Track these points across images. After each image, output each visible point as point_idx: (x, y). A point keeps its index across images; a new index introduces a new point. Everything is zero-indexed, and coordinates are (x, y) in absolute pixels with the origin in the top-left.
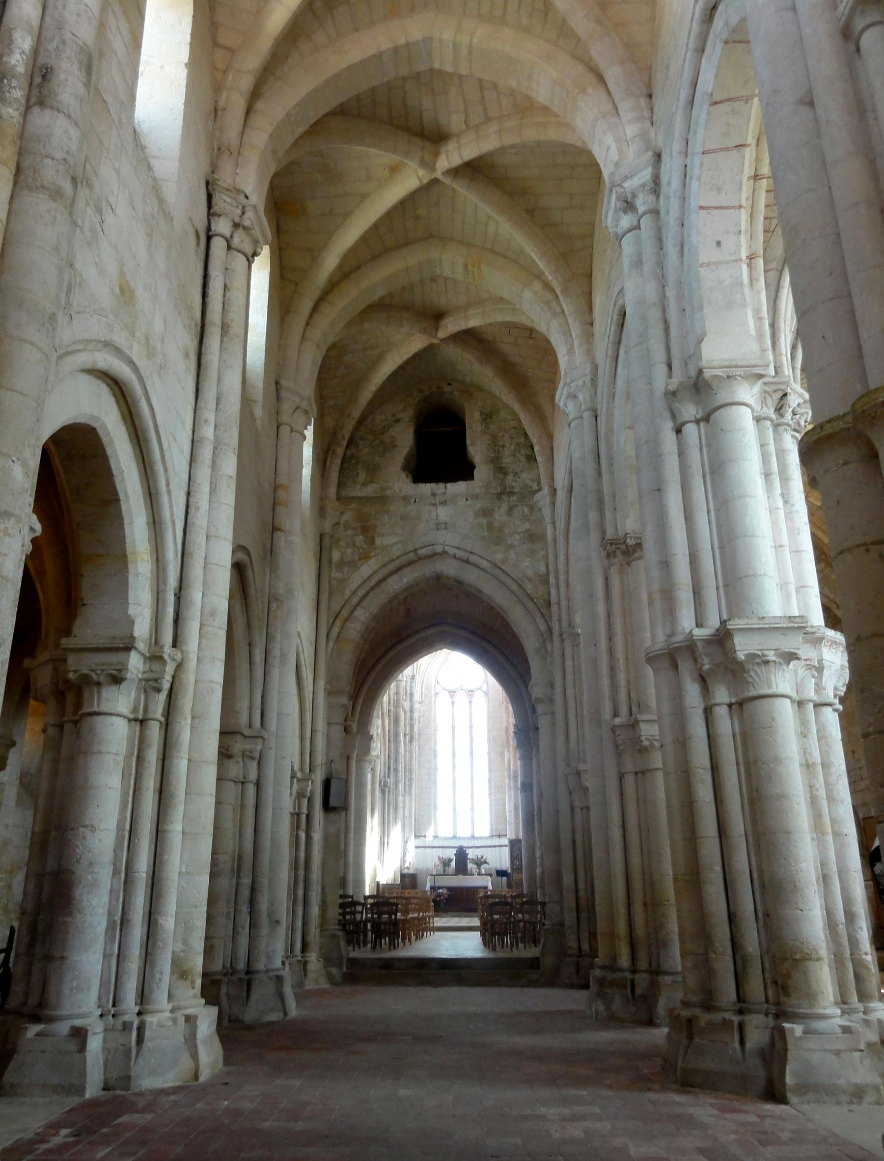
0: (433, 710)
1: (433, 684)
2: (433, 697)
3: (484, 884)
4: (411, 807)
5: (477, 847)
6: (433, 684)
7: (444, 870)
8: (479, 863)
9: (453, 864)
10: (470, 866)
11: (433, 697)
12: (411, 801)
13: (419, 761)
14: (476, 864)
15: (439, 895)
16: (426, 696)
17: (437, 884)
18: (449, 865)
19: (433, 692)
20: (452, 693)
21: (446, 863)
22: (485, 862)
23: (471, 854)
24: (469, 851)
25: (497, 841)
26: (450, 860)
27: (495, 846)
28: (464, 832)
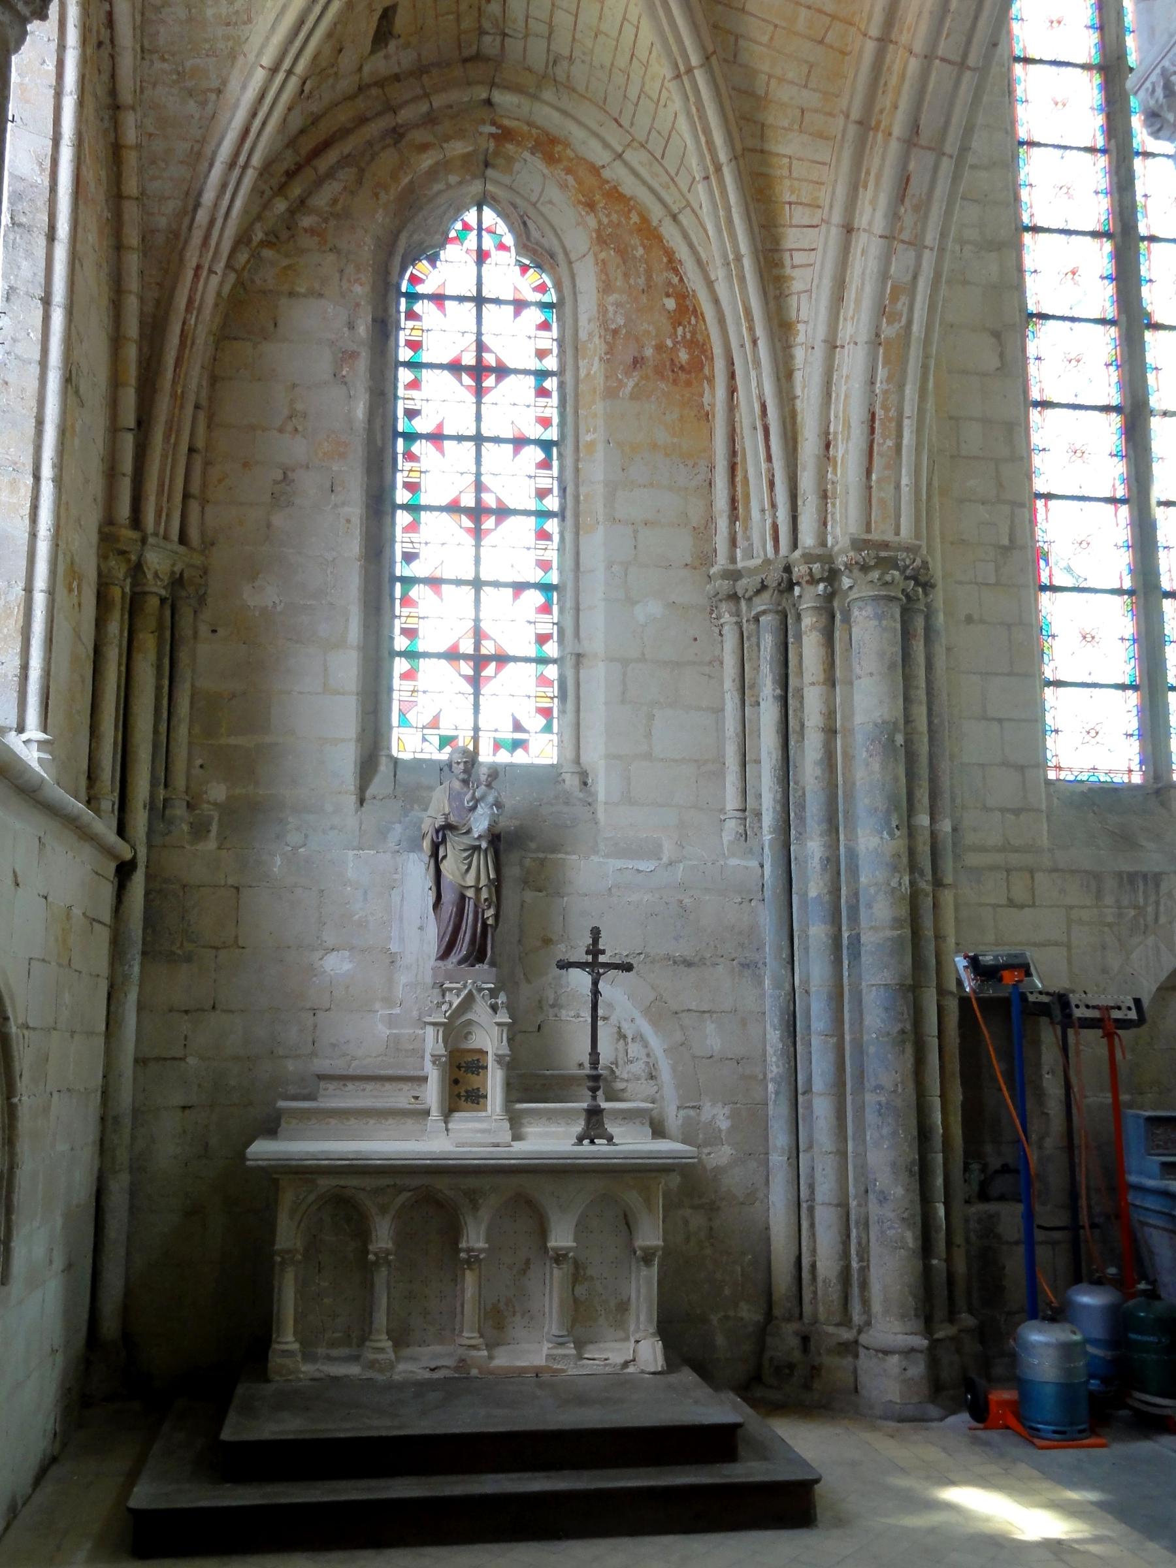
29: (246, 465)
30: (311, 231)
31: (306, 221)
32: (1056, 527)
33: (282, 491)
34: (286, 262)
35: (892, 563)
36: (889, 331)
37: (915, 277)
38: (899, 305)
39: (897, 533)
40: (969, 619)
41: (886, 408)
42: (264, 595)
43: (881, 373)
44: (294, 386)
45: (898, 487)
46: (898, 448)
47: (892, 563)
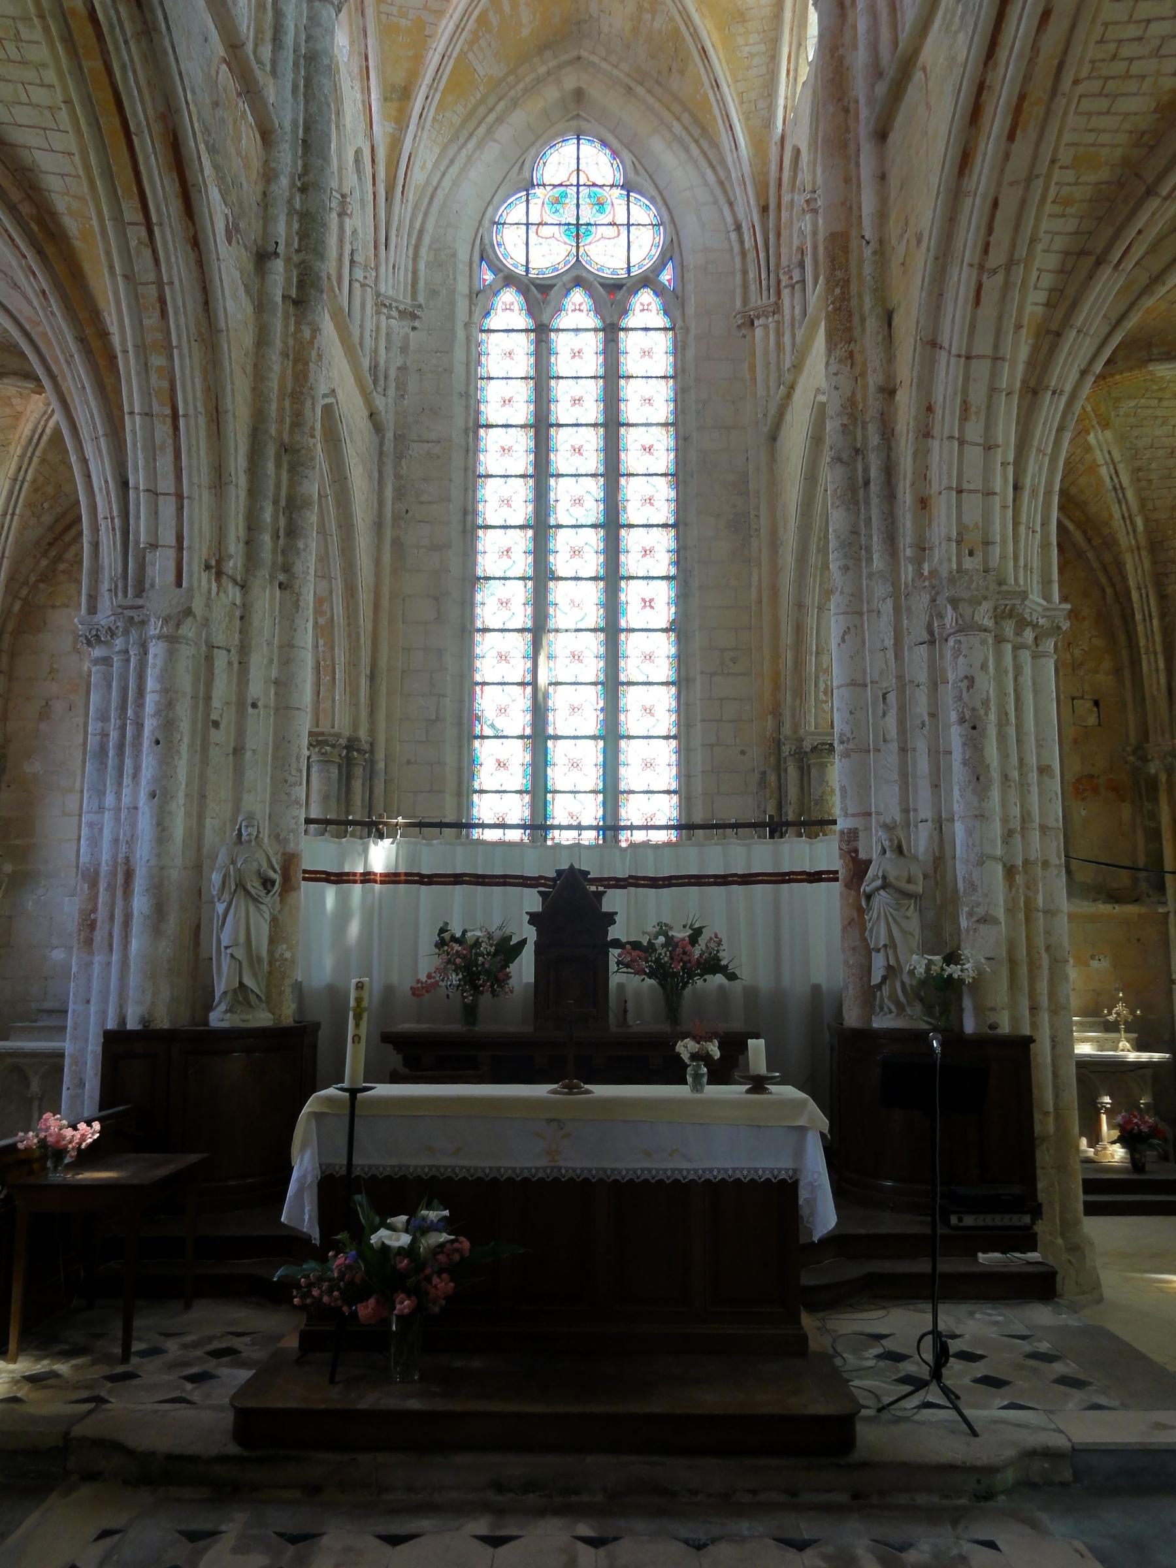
0: (459, 354)
1: (463, 255)
2: (462, 306)
3: (761, 1160)
4: (288, 647)
5: (655, 883)
6: (463, 255)
7: (470, 1012)
8: (680, 965)
9: (524, 970)
10: (617, 978)
11: (462, 306)
12: (289, 614)
13: (397, 544)
14: (660, 972)
15: (385, 1275)
16: (433, 293)
17: (377, 1155)
18: (499, 979)
19: (462, 287)
20: (541, 295)
21: (476, 965)
22: (712, 965)
23: (632, 917)
24: (614, 900)
25: (759, 855)
26: (508, 950)
27: (747, 879)
28: (575, 811)
29: (28, 699)
30: (63, 572)
31: (62, 567)
32: (487, 702)
33: (45, 713)
34: (51, 589)
35: (326, 743)
36: (321, 621)
37: (331, 593)
38: (324, 608)
39: (333, 727)
40: (408, 762)
41: (325, 660)
42: (34, 767)
43: (321, 642)
44: (53, 655)
45: (334, 701)
46: (334, 679)
47: (326, 743)
